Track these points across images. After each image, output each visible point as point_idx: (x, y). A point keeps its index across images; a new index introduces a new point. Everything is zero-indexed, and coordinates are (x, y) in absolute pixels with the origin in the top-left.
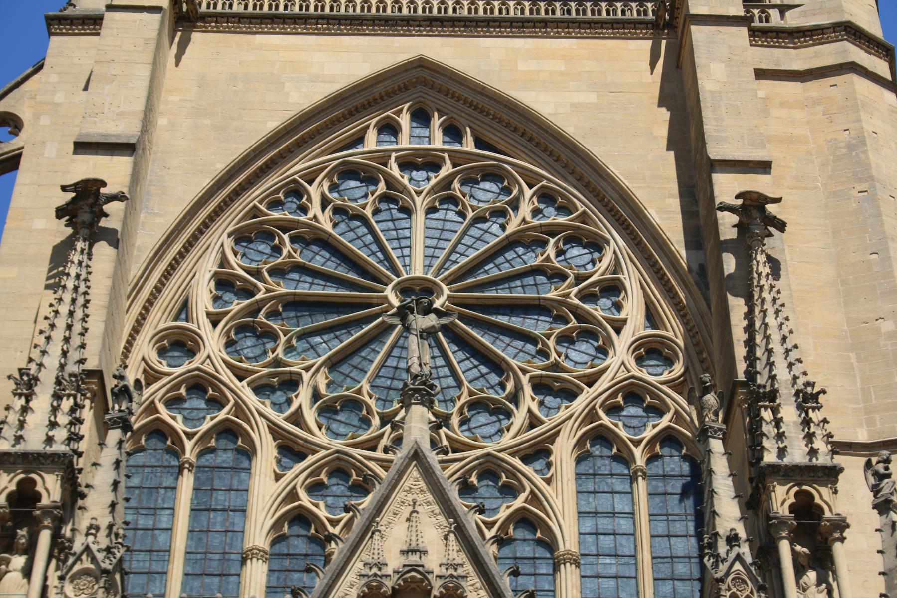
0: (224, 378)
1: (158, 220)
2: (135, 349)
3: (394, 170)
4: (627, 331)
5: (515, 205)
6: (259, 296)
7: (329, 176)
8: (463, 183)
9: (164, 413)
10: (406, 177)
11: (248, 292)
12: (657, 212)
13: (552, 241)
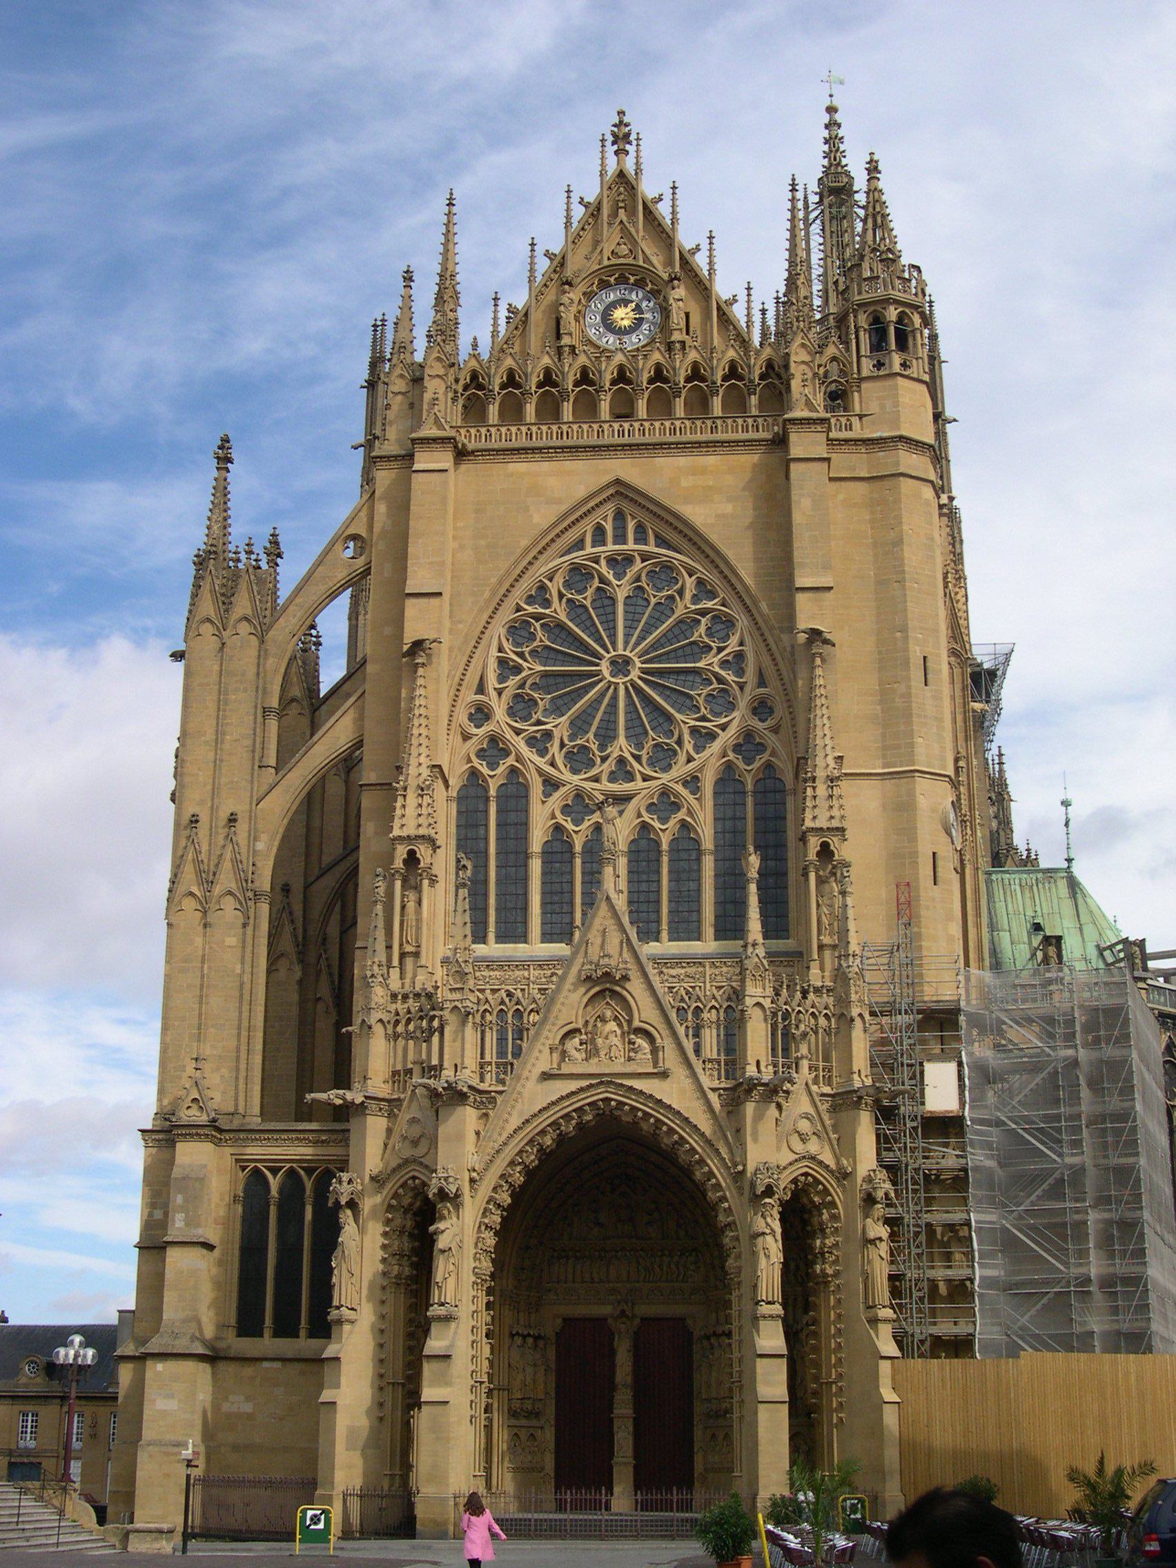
0: (508, 737)
1: (460, 626)
2: (454, 719)
3: (604, 568)
4: (748, 689)
5: (681, 592)
6: (524, 674)
9: (476, 762)
10: (612, 572)
11: (518, 669)
13: (703, 620)
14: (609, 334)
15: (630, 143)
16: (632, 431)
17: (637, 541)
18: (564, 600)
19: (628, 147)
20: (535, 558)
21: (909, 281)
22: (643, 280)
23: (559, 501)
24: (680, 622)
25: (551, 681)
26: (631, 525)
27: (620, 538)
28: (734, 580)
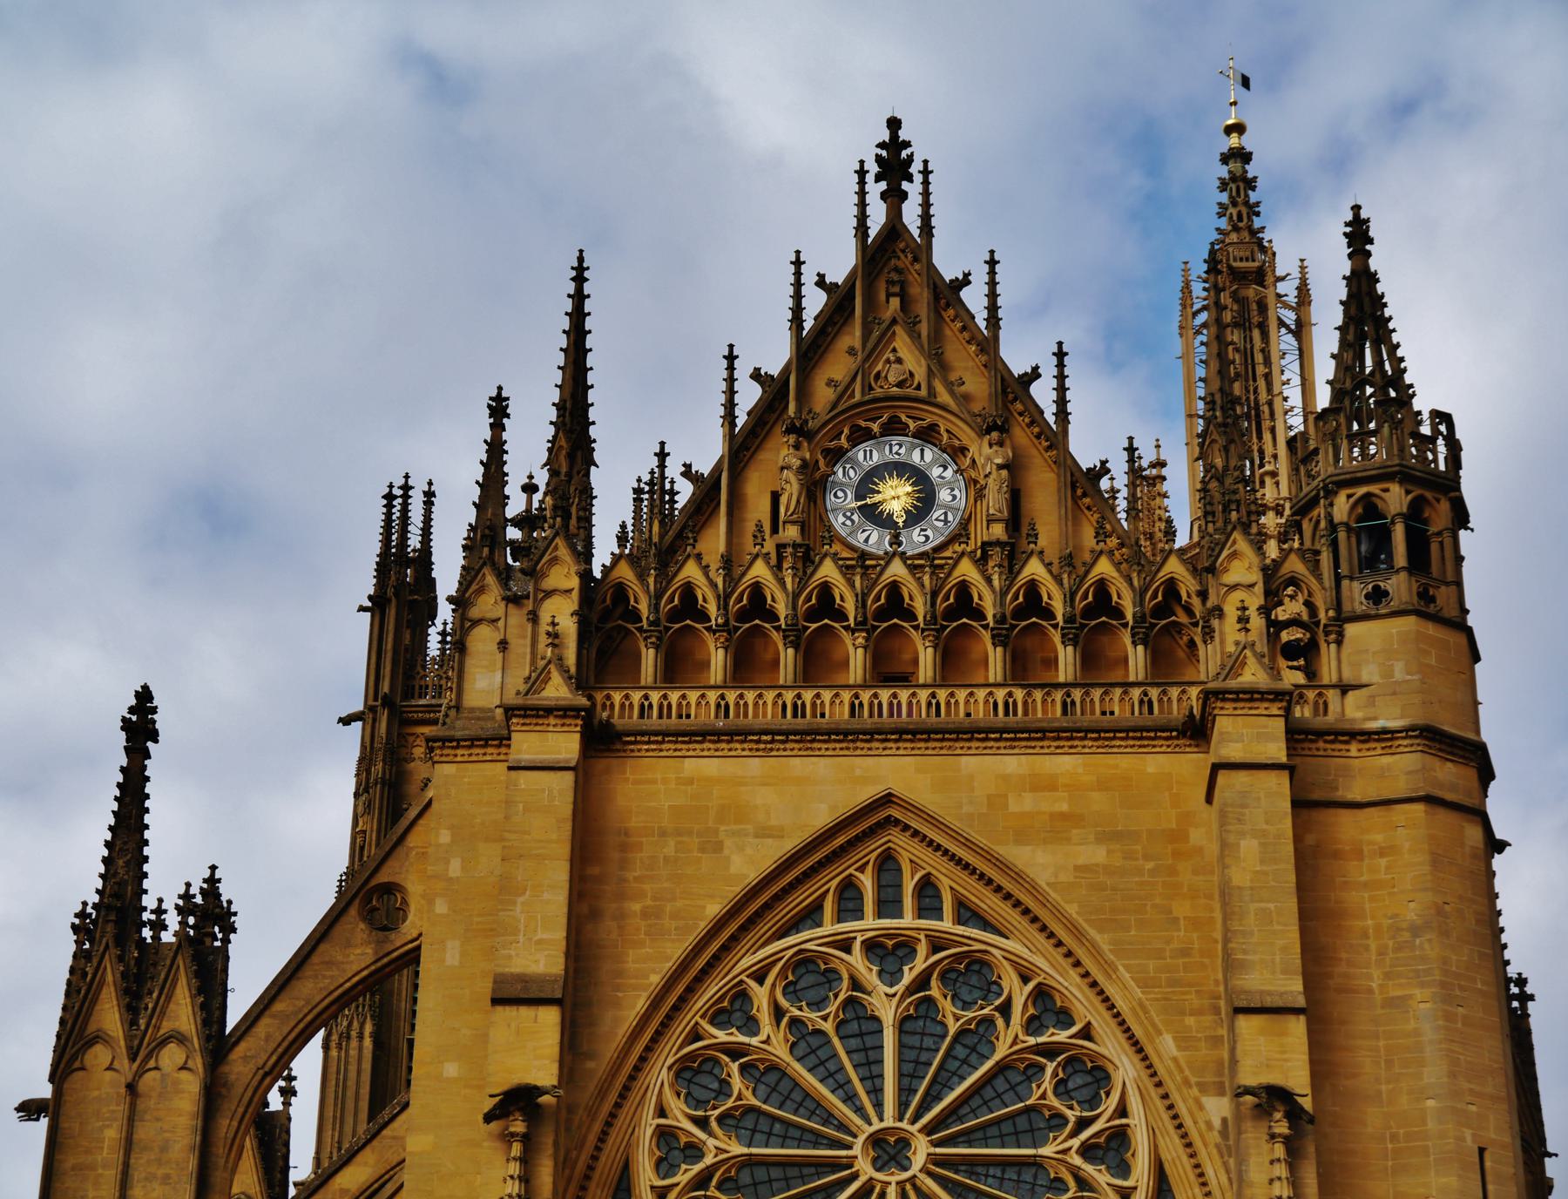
1: (590, 1065)
5: (1005, 1010)
7: (782, 974)
8: (943, 977)
12: (1175, 1039)
14: (869, 526)
15: (910, 179)
16: (914, 703)
17: (921, 913)
18: (785, 1020)
19: (905, 185)
20: (734, 939)
21: (1432, 440)
22: (933, 427)
23: (777, 833)
24: (1002, 1068)
25: (761, 1173)
26: (909, 886)
27: (888, 905)
28: (1111, 990)
